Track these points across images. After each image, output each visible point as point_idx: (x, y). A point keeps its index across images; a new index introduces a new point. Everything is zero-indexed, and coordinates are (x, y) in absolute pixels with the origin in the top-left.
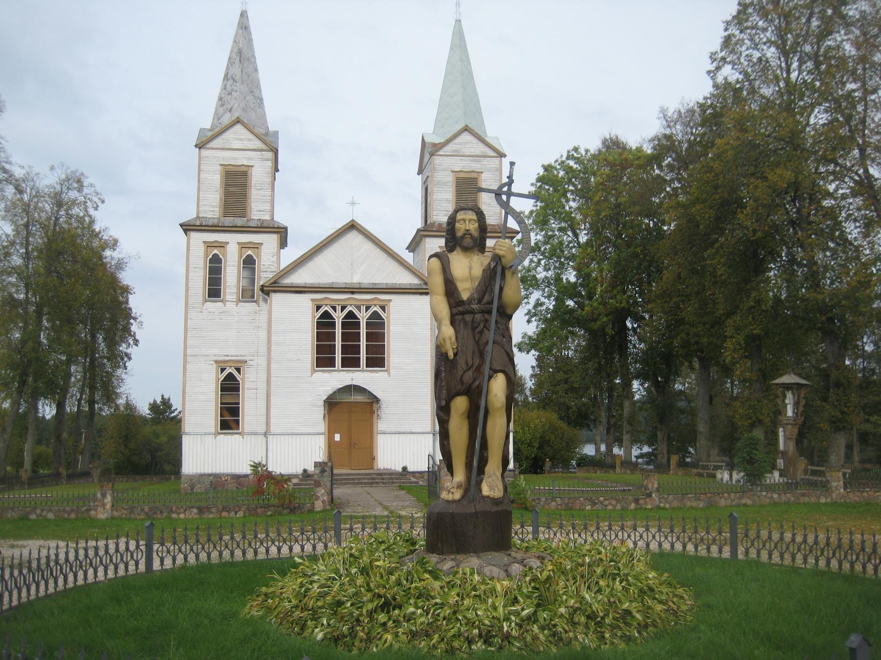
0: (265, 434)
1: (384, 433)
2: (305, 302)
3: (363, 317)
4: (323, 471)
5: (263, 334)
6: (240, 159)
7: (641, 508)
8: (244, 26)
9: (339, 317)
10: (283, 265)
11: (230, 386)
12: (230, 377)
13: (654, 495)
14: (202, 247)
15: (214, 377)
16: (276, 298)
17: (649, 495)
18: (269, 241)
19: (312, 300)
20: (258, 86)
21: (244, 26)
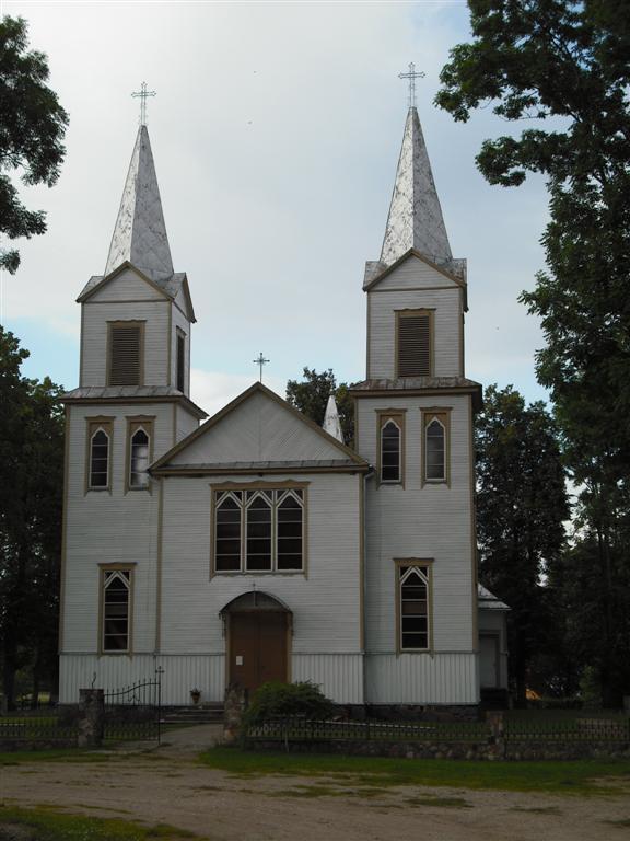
0: (155, 657)
1: (300, 654)
2: (201, 490)
3: (274, 505)
4: (89, 700)
5: (155, 529)
6: (129, 313)
7: (482, 759)
8: (144, 146)
9: (244, 505)
10: (180, 438)
11: (116, 595)
12: (117, 583)
13: (497, 741)
14: (84, 424)
15: (96, 583)
16: (171, 485)
17: (492, 741)
18: (162, 414)
19: (211, 485)
20: (161, 219)
21: (144, 146)
